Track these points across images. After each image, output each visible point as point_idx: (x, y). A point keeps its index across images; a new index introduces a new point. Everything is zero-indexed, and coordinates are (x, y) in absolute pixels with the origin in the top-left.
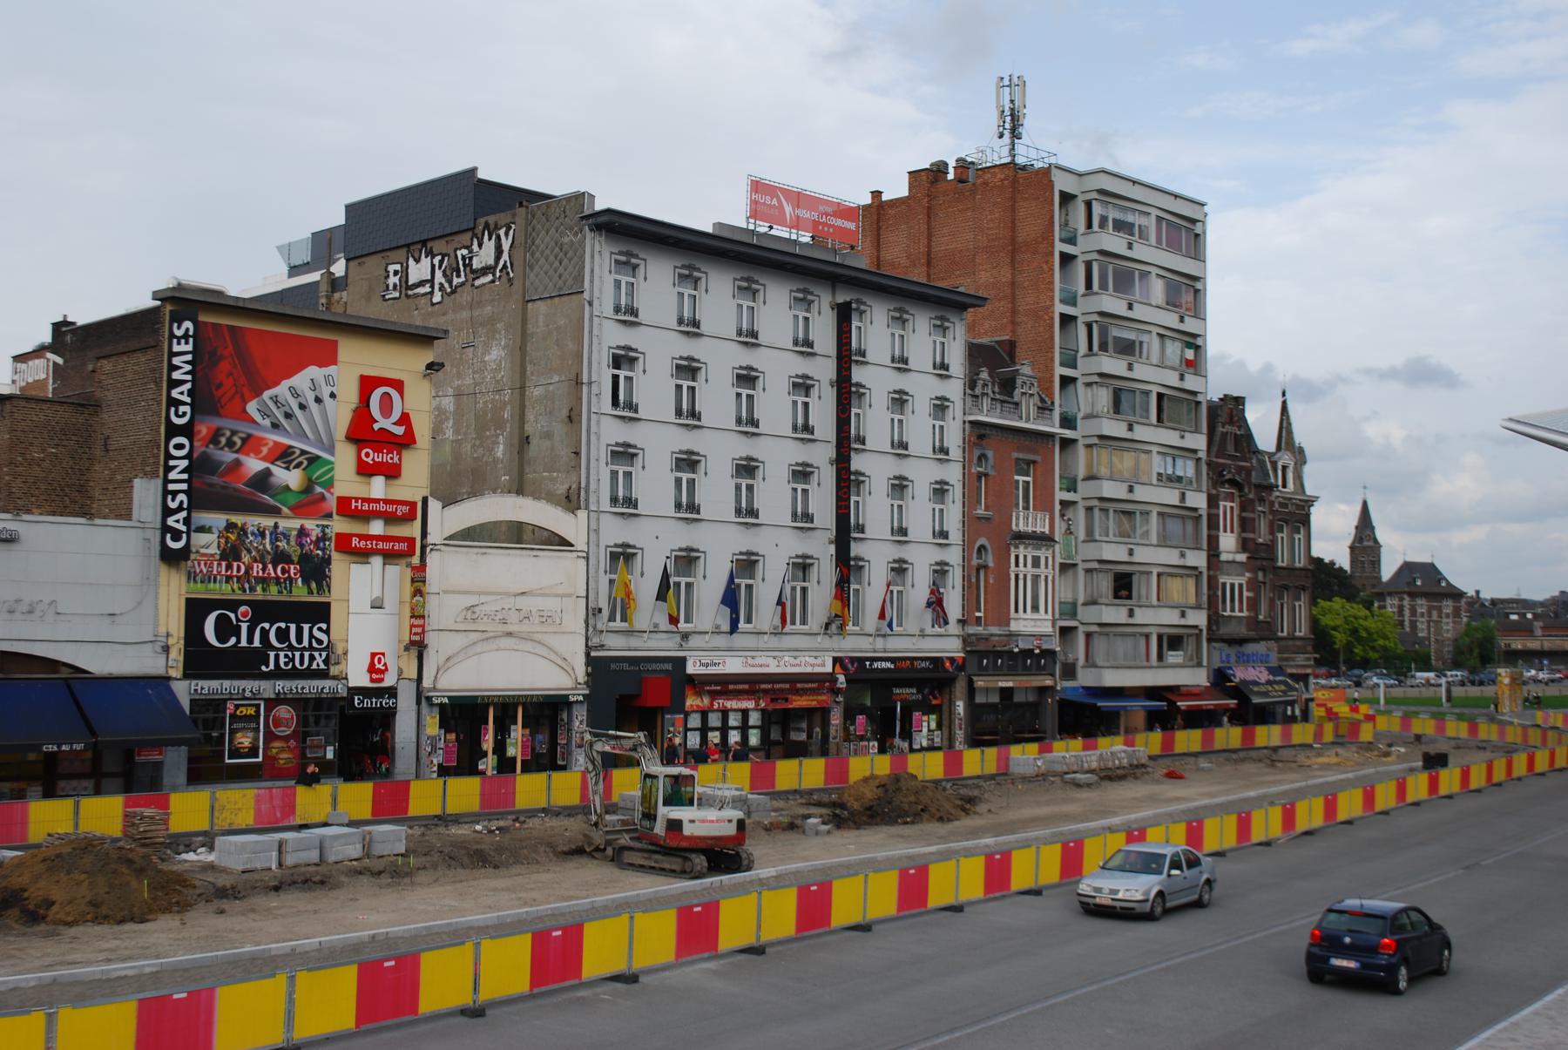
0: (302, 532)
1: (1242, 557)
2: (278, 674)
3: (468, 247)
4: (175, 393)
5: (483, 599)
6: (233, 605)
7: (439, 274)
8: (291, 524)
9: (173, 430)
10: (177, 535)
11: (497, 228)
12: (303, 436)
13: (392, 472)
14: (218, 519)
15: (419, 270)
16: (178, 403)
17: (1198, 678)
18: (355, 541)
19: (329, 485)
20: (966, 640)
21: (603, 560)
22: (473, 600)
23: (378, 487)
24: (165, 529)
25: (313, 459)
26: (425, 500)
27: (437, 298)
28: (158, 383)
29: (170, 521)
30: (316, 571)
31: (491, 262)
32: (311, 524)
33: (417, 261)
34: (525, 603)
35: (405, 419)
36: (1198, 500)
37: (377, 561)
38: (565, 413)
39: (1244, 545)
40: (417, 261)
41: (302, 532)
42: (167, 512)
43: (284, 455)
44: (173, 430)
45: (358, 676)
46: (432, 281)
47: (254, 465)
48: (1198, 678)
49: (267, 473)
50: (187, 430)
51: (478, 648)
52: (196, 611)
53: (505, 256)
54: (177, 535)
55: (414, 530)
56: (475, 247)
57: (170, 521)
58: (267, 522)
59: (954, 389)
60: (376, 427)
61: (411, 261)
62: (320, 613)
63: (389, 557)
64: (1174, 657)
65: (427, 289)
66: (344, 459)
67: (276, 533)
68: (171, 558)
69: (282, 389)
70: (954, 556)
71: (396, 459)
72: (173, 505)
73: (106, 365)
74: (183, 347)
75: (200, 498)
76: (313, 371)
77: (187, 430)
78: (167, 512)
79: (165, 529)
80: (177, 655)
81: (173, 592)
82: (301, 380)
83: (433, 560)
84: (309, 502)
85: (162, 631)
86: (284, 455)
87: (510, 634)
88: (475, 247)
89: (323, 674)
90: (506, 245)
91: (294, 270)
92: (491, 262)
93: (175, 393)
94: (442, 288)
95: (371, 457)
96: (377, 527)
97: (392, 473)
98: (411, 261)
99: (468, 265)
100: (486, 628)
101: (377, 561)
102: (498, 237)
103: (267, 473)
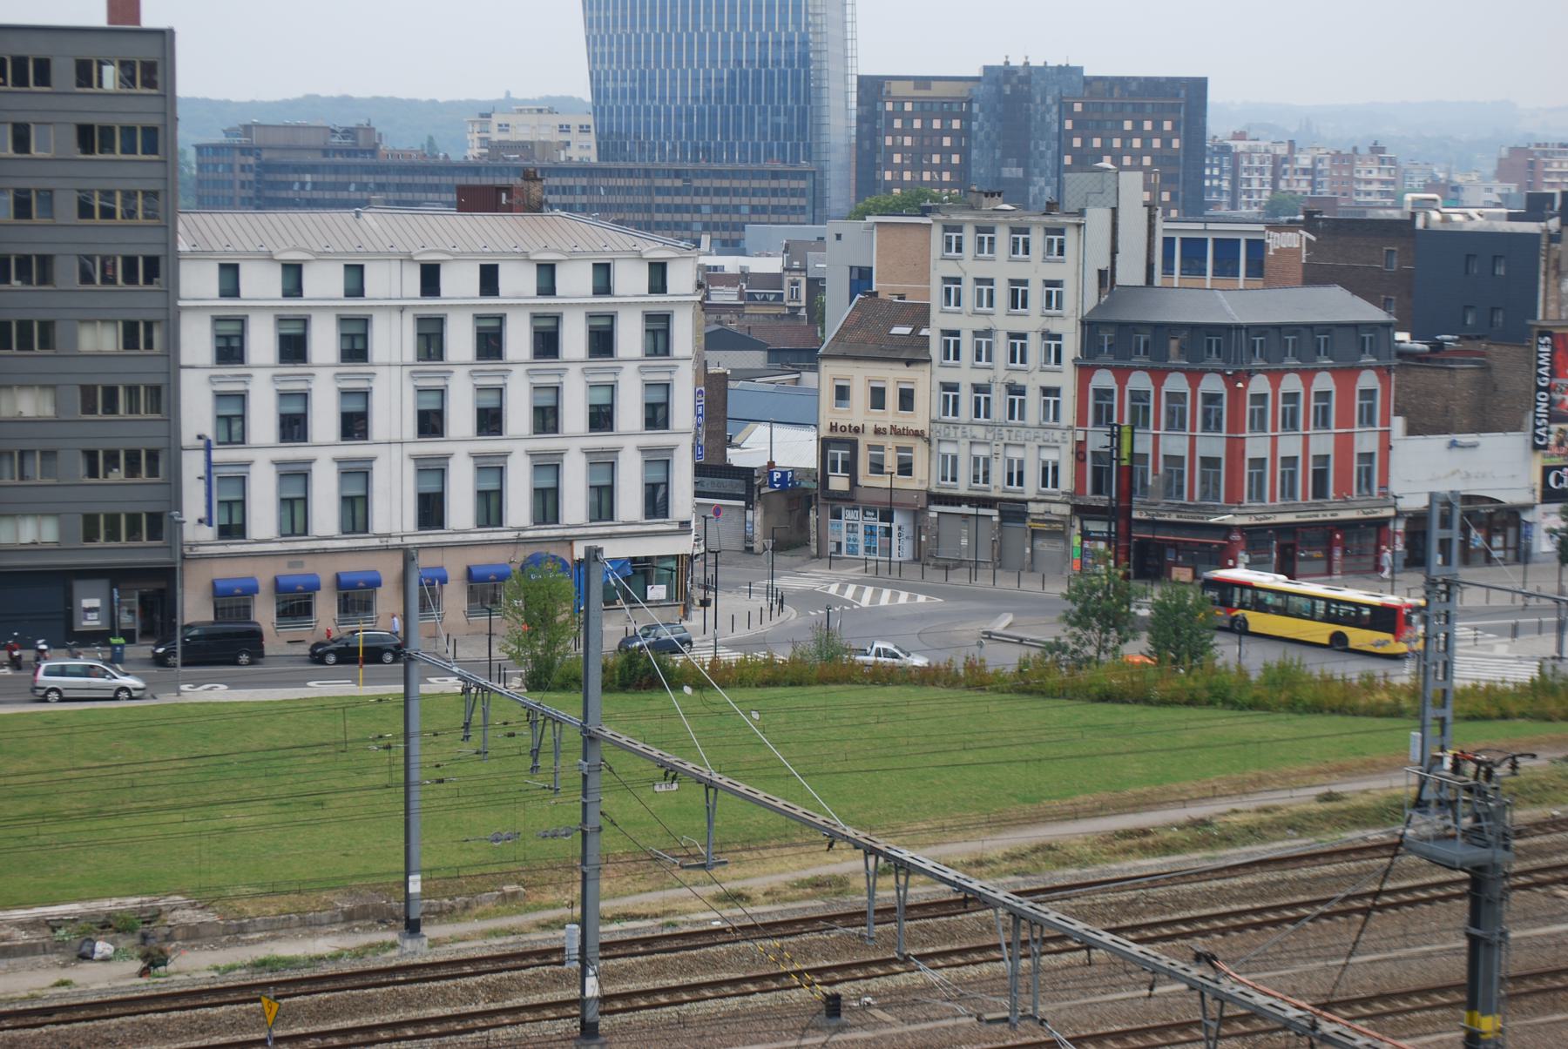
4: (1540, 371)
9: (1539, 389)
10: (1541, 438)
14: (1554, 427)
44: (1539, 389)
50: (1547, 389)
52: (1546, 471)
54: (1541, 438)
68: (1536, 447)
73: (1495, 349)
75: (1553, 418)
77: (1547, 389)
78: (1537, 427)
79: (1536, 435)
80: (1538, 494)
81: (1538, 462)
93: (1540, 371)
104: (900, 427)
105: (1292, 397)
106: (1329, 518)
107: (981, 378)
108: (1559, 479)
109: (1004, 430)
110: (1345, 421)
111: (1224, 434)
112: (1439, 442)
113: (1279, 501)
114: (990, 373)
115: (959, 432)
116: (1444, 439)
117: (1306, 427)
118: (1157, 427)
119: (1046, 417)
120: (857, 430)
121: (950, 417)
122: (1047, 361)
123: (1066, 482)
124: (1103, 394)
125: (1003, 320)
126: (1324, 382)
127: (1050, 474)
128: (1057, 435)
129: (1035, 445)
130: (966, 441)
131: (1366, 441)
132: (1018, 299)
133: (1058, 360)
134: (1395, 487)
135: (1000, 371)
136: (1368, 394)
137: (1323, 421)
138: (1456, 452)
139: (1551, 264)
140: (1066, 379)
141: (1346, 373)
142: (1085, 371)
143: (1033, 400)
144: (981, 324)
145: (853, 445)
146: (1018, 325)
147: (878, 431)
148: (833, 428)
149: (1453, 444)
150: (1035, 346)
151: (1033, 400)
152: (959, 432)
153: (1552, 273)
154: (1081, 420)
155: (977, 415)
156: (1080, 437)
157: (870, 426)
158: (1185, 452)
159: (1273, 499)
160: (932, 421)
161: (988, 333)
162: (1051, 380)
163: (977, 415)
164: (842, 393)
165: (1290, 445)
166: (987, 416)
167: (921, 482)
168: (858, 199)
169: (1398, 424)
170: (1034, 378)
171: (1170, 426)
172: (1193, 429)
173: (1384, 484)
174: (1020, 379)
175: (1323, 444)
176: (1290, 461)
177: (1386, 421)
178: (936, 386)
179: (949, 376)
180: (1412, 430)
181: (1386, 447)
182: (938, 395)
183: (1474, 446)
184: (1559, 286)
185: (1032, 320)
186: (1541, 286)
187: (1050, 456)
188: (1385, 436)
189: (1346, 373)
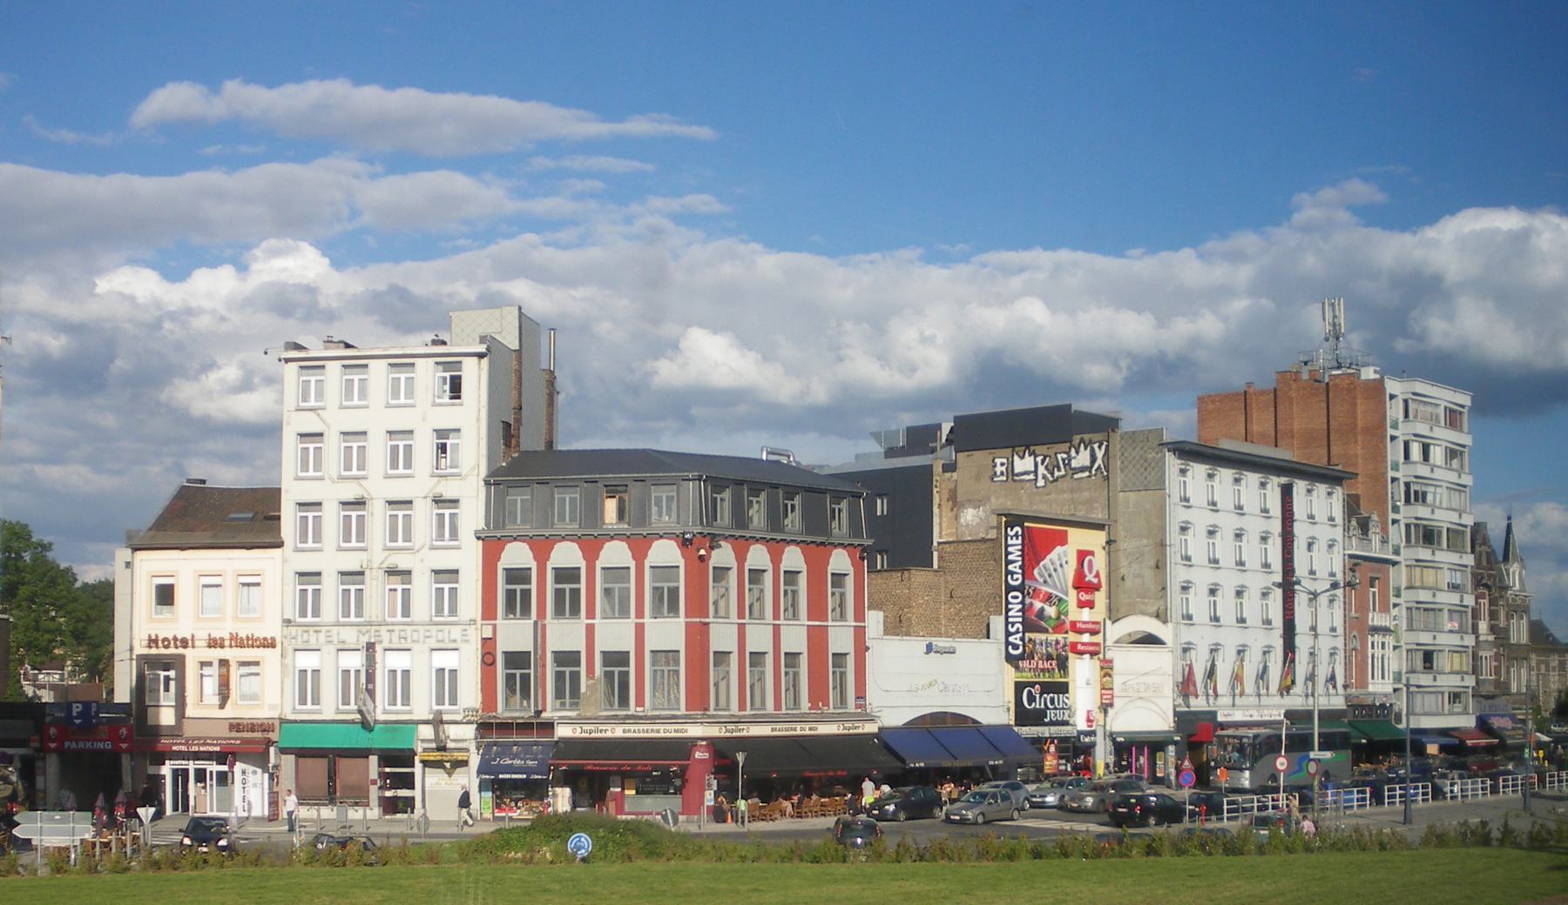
0: (1057, 642)
1: (1491, 638)
2: (1052, 723)
3: (1068, 453)
4: (1010, 567)
6: (1032, 685)
7: (1041, 470)
8: (1052, 637)
9: (1009, 589)
10: (1016, 647)
11: (1091, 442)
12: (1055, 587)
15: (1024, 464)
16: (1012, 573)
17: (1468, 722)
19: (1066, 614)
20: (1347, 698)
21: (1180, 651)
24: (1008, 643)
25: (1060, 600)
27: (1041, 483)
28: (997, 561)
29: (1011, 639)
30: (1063, 665)
31: (1088, 463)
32: (1060, 637)
33: (1022, 458)
34: (1149, 680)
35: (1097, 575)
36: (1469, 600)
37: (1087, 656)
38: (1153, 563)
39: (1493, 629)
40: (1022, 458)
41: (1057, 642)
42: (1008, 634)
43: (1048, 598)
44: (1009, 589)
45: (1082, 725)
46: (1036, 472)
47: (1038, 605)
48: (1468, 722)
49: (1042, 610)
50: (1020, 588)
52: (1019, 687)
53: (1099, 462)
54: (1016, 647)
56: (1073, 453)
57: (1011, 639)
58: (1043, 637)
59: (1338, 533)
61: (1016, 458)
62: (1063, 688)
63: (1093, 654)
64: (1458, 708)
65: (1032, 477)
66: (1072, 597)
67: (1048, 644)
69: (1046, 561)
70: (1340, 643)
72: (1012, 630)
74: (1014, 541)
76: (1059, 549)
77: (1020, 588)
81: (1010, 676)
82: (1054, 555)
84: (1059, 628)
86: (1048, 598)
88: (1073, 453)
89: (1065, 723)
90: (1100, 454)
91: (891, 453)
92: (1088, 463)
93: (1010, 567)
94: (1044, 477)
95: (1084, 597)
97: (1090, 605)
98: (1016, 458)
99: (1067, 464)
101: (1087, 656)
102: (1093, 450)
103: (1042, 610)
104: (243, 634)
106: (807, 732)
107: (352, 562)
108: (1031, 699)
109: (383, 629)
111: (682, 619)
112: (917, 645)
114: (363, 556)
115: (322, 636)
116: (919, 645)
119: (439, 611)
120: (184, 643)
121: (309, 619)
122: (441, 536)
123: (470, 695)
124: (517, 576)
125: (379, 487)
126: (793, 558)
127: (446, 682)
128: (456, 632)
129: (426, 648)
130: (332, 649)
132: (400, 457)
133: (454, 534)
134: (873, 697)
135: (376, 553)
139: (945, 496)
140: (468, 558)
142: (492, 545)
143: (422, 588)
144: (350, 492)
145: (177, 663)
146: (399, 490)
147: (214, 643)
148: (153, 642)
150: (423, 514)
151: (422, 588)
152: (322, 636)
153: (947, 506)
154: (489, 612)
155: (346, 614)
156: (488, 633)
157: (201, 636)
158: (628, 645)
160: (287, 622)
161: (359, 503)
162: (445, 561)
163: (346, 614)
164: (165, 595)
166: (359, 614)
167: (272, 707)
169: (874, 620)
170: (422, 563)
172: (640, 614)
173: (861, 695)
174: (403, 562)
177: (860, 616)
178: (291, 578)
179: (308, 563)
181: (861, 648)
182: (292, 587)
184: (957, 518)
185: (420, 484)
186: (936, 520)
187: (447, 660)
188: (860, 633)
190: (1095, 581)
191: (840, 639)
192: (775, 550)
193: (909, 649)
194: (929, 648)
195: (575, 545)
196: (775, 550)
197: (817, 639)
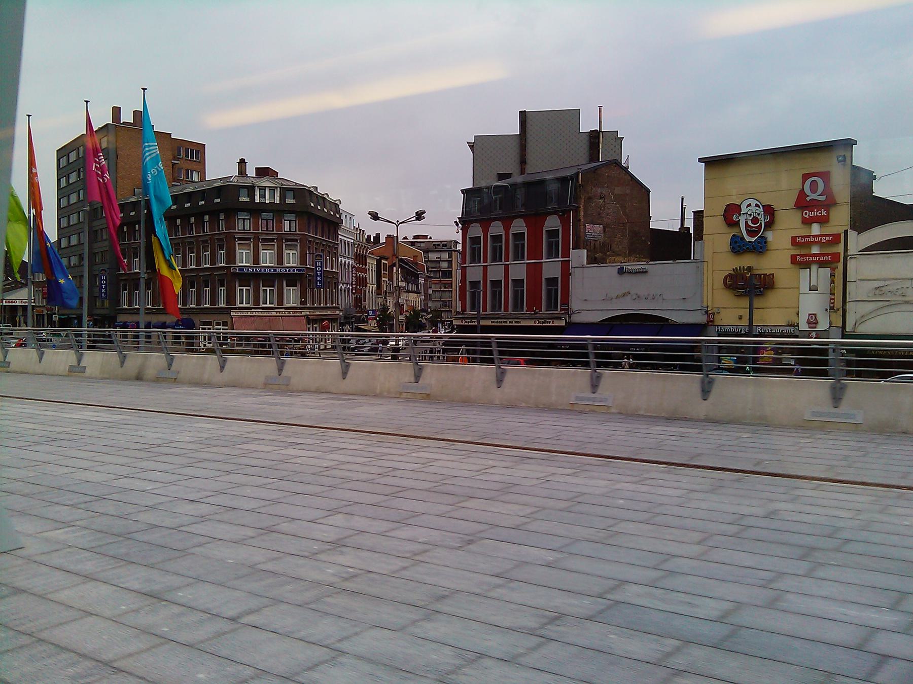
5: (887, 283)
13: (823, 221)
18: (798, 258)
22: (881, 284)
23: (816, 229)
26: (846, 232)
37: (814, 268)
51: (879, 312)
55: (840, 249)
60: (808, 199)
63: (822, 264)
71: (824, 213)
83: (851, 265)
85: (705, 305)
87: (907, 302)
95: (808, 214)
96: (815, 250)
100: (887, 297)
101: (814, 268)
105: (497, 238)
110: (535, 253)
113: (510, 311)
117: (507, 260)
118: (485, 261)
126: (519, 226)
131: (551, 268)
134: (575, 305)
136: (553, 234)
137: (519, 256)
138: (626, 278)
141: (535, 219)
149: (621, 271)
159: (506, 309)
165: (496, 272)
168: (163, 137)
169: (579, 256)
171: (494, 259)
175: (519, 270)
176: (496, 284)
177: (566, 254)
180: (593, 260)
183: (646, 272)
188: (565, 266)
189: (535, 219)
190: (823, 198)
191: (551, 268)
192: (507, 223)
193: (606, 273)
194: (621, 271)
195: (478, 225)
196: (507, 223)
197: (535, 271)
